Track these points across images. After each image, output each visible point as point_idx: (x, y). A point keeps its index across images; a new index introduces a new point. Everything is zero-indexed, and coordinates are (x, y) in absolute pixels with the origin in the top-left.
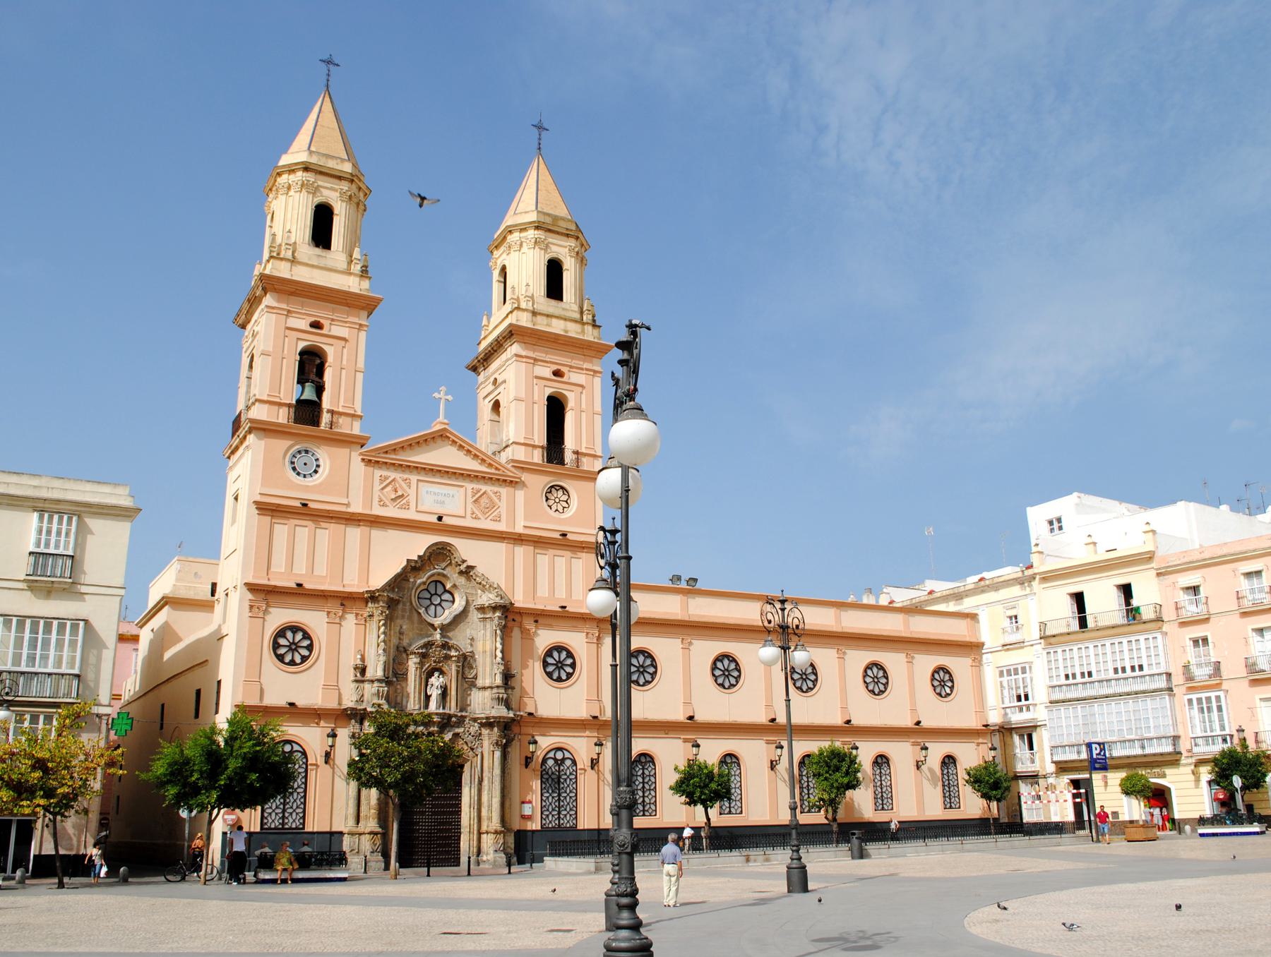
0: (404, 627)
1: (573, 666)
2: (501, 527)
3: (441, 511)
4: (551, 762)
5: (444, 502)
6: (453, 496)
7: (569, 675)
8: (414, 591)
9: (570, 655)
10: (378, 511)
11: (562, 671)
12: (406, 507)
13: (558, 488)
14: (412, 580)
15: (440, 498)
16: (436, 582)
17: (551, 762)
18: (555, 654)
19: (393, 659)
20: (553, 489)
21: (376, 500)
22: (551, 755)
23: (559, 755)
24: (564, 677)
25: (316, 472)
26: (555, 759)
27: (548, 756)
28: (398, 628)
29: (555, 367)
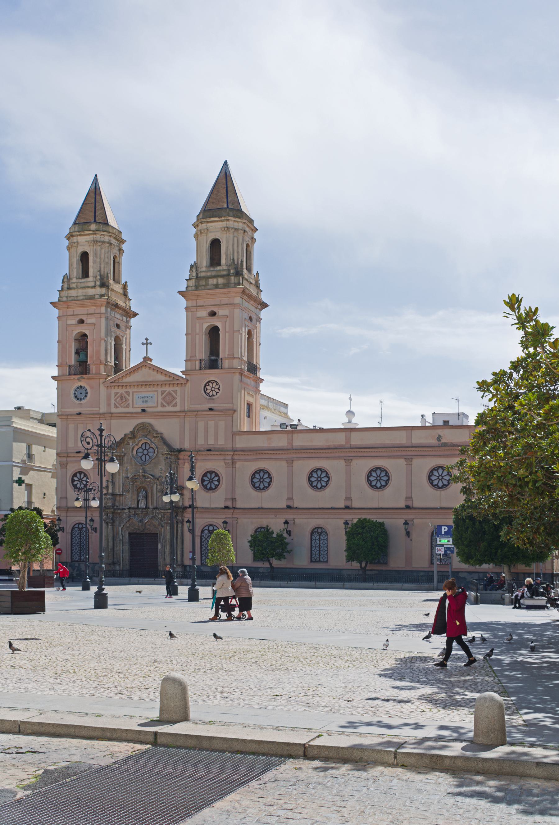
0: (128, 468)
1: (219, 481)
2: (177, 409)
3: (144, 405)
4: (206, 532)
5: (147, 401)
6: (152, 397)
7: (217, 486)
8: (131, 450)
9: (217, 475)
10: (113, 410)
11: (212, 484)
12: (128, 406)
13: (213, 382)
14: (131, 444)
15: (145, 399)
16: (146, 443)
17: (206, 532)
18: (209, 475)
19: (123, 484)
20: (210, 383)
21: (113, 405)
22: (207, 528)
23: (211, 528)
24: (214, 487)
25: (76, 397)
26: (209, 531)
27: (204, 529)
28: (125, 469)
29: (209, 310)
